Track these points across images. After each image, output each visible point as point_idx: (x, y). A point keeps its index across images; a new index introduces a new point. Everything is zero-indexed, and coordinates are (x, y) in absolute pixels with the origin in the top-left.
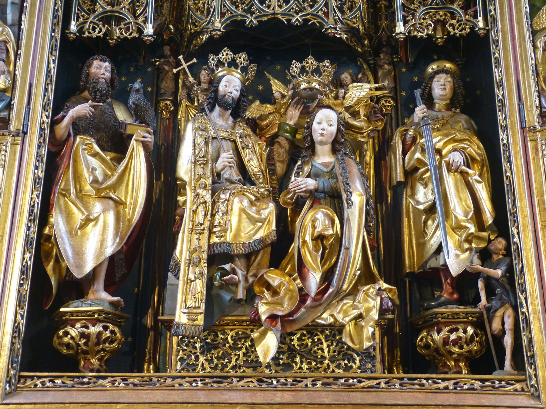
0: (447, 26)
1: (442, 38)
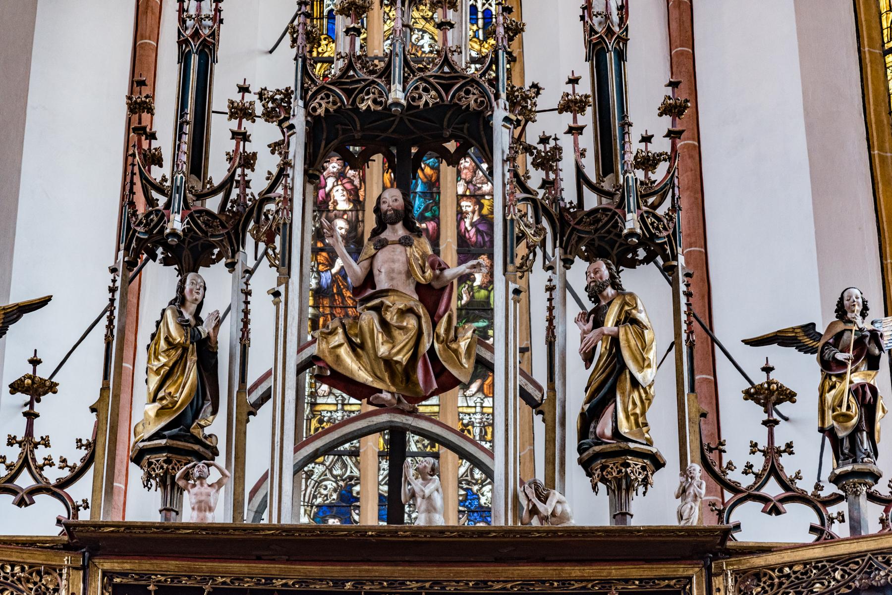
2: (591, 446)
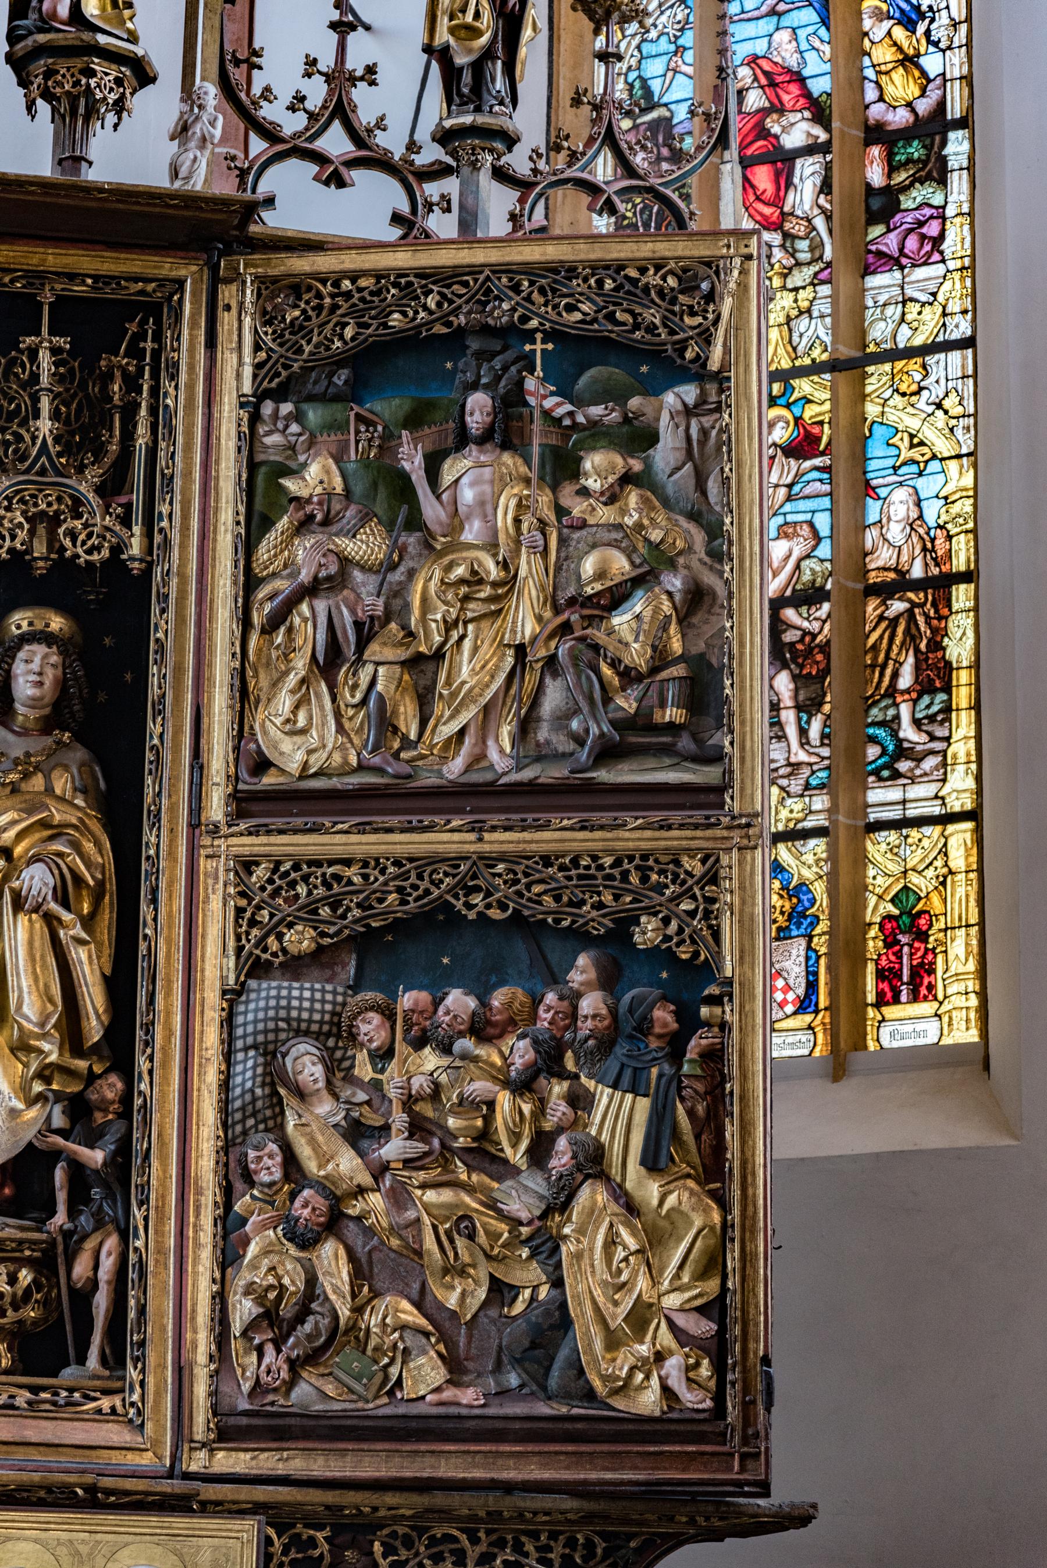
0: (61, 531)
1: (46, 559)
2: (31, 33)
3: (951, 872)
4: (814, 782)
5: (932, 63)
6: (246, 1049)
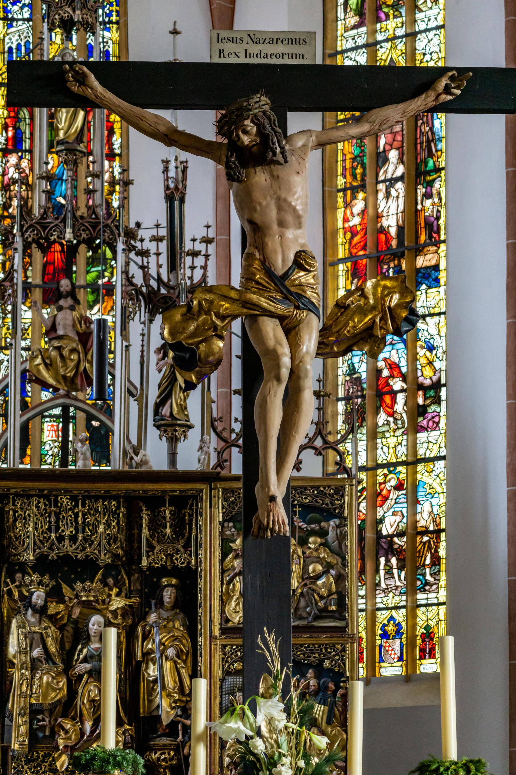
3: (440, 620)
4: (402, 592)
5: (437, 364)
6: (226, 694)
